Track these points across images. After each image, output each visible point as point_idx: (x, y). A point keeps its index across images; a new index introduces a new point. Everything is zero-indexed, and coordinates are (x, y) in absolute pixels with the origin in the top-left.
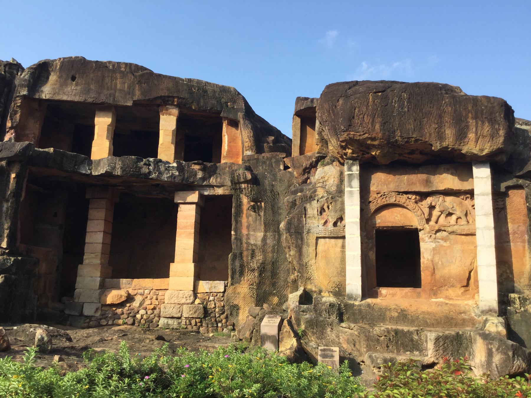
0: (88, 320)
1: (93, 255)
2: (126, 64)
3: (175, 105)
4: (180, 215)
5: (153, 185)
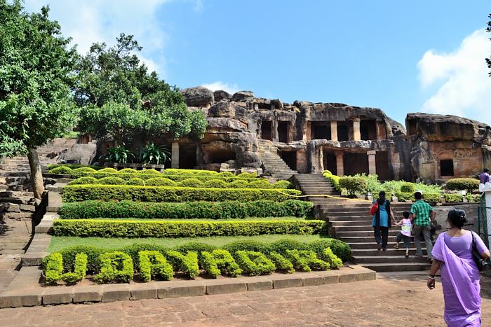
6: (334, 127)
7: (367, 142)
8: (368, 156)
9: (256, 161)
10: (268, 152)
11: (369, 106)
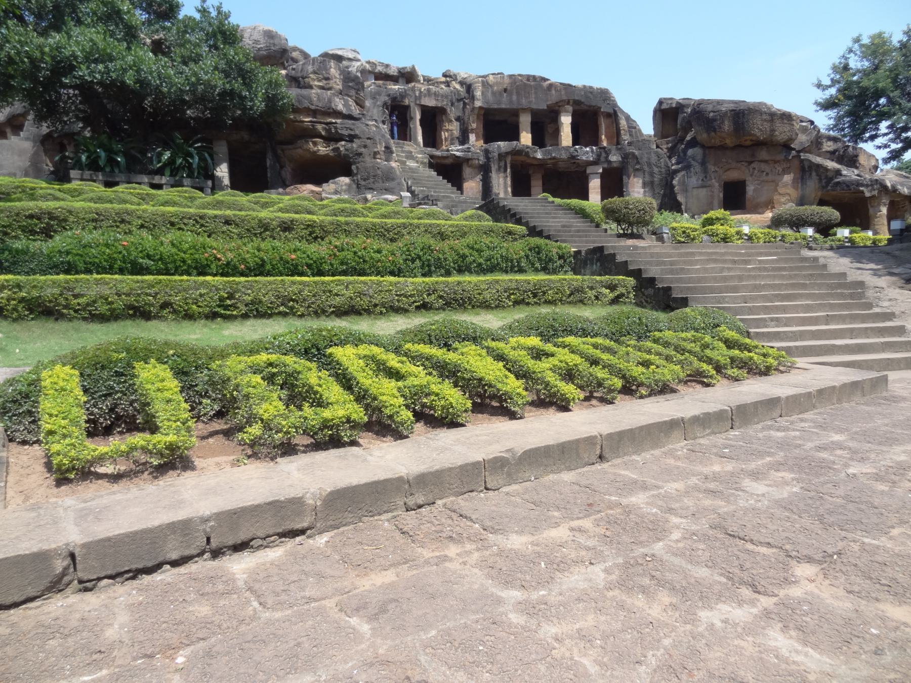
7: (588, 149)
9: (393, 179)
10: (412, 164)
11: (588, 83)
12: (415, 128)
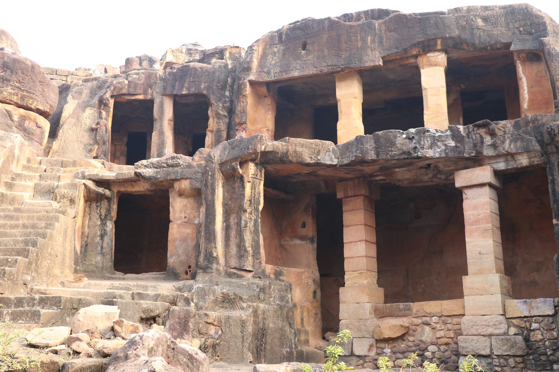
0: (361, 362)
1: (356, 274)
2: (366, 13)
3: (438, 51)
4: (466, 204)
5: (421, 168)
6: (350, 100)
8: (454, 198)
12: (161, 133)
